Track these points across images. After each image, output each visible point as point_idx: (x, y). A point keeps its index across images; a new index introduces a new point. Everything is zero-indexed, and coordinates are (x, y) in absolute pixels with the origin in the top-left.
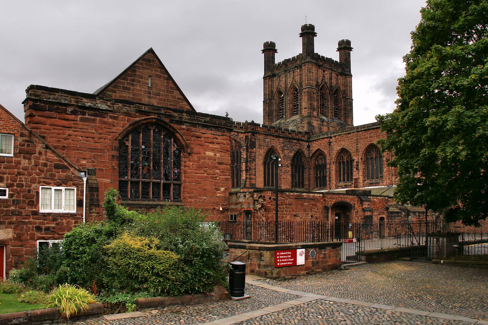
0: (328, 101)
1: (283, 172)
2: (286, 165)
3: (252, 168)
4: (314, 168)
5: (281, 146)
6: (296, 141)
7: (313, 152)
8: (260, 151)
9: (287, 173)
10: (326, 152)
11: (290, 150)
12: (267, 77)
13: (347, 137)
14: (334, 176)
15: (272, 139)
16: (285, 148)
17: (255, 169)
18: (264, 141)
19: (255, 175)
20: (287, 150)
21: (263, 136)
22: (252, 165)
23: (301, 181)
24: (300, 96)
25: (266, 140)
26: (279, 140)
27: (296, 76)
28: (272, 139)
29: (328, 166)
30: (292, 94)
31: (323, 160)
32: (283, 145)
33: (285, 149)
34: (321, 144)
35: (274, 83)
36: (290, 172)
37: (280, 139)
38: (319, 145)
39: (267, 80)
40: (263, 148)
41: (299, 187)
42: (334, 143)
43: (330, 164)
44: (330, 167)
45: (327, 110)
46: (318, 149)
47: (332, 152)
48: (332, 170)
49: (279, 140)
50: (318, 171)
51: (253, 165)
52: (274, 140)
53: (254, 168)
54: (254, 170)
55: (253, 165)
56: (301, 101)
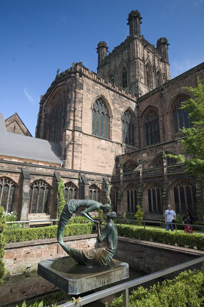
0: (152, 77)
1: (114, 124)
2: (116, 118)
3: (77, 109)
4: (144, 127)
5: (111, 98)
6: (126, 99)
7: (143, 110)
8: (89, 96)
9: (117, 126)
10: (157, 106)
11: (121, 105)
12: (100, 66)
13: (183, 82)
14: (169, 127)
15: (102, 89)
16: (115, 101)
17: (82, 111)
18: (93, 88)
19: (81, 118)
20: (117, 104)
21: (92, 82)
22: (78, 106)
23: (132, 139)
24: (128, 69)
25: (96, 87)
26: (109, 92)
27: (124, 56)
28: (102, 89)
29: (161, 119)
30: (120, 73)
31: (154, 116)
32: (113, 98)
33: (115, 103)
34: (151, 100)
35: (105, 70)
36: (121, 126)
37: (110, 91)
38: (149, 102)
39: (100, 69)
40: (92, 94)
41: (130, 144)
42: (167, 94)
43: (163, 116)
44: (163, 119)
45: (151, 84)
46: (149, 106)
47: (164, 104)
48: (166, 121)
49: (109, 92)
50: (149, 129)
51: (80, 106)
52: (105, 90)
53: (80, 110)
54: (80, 112)
55: (80, 106)
56: (129, 73)
